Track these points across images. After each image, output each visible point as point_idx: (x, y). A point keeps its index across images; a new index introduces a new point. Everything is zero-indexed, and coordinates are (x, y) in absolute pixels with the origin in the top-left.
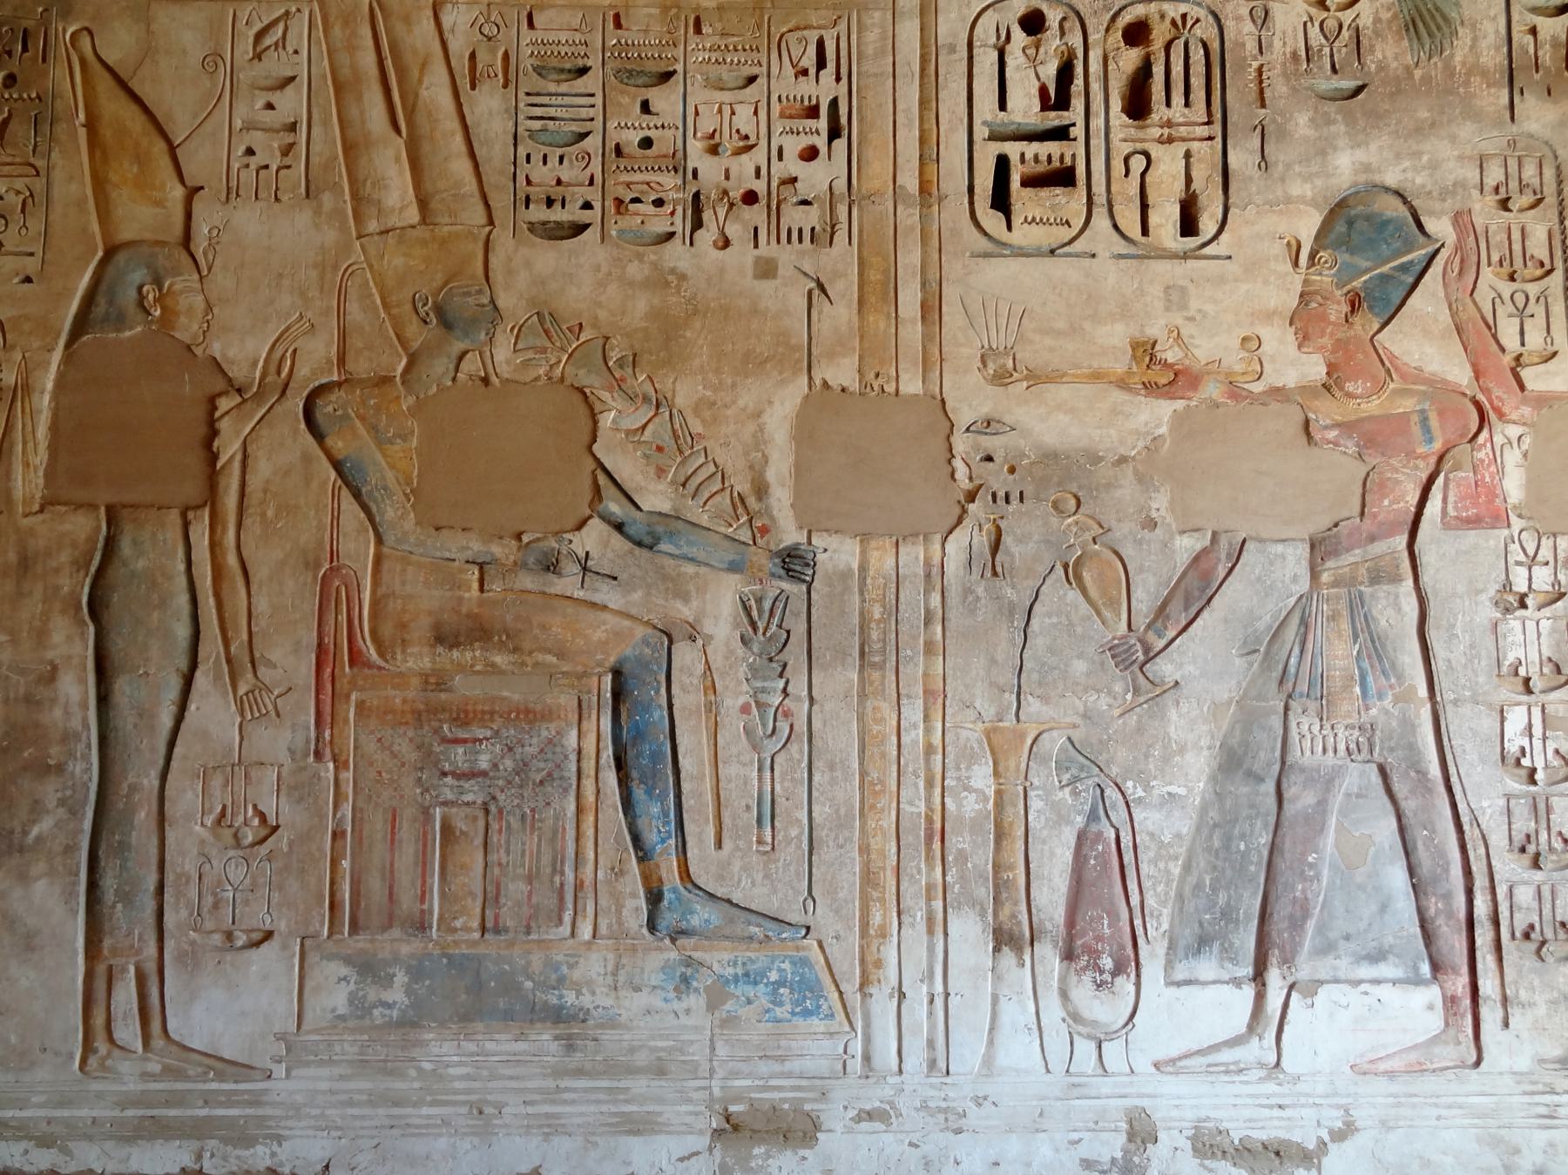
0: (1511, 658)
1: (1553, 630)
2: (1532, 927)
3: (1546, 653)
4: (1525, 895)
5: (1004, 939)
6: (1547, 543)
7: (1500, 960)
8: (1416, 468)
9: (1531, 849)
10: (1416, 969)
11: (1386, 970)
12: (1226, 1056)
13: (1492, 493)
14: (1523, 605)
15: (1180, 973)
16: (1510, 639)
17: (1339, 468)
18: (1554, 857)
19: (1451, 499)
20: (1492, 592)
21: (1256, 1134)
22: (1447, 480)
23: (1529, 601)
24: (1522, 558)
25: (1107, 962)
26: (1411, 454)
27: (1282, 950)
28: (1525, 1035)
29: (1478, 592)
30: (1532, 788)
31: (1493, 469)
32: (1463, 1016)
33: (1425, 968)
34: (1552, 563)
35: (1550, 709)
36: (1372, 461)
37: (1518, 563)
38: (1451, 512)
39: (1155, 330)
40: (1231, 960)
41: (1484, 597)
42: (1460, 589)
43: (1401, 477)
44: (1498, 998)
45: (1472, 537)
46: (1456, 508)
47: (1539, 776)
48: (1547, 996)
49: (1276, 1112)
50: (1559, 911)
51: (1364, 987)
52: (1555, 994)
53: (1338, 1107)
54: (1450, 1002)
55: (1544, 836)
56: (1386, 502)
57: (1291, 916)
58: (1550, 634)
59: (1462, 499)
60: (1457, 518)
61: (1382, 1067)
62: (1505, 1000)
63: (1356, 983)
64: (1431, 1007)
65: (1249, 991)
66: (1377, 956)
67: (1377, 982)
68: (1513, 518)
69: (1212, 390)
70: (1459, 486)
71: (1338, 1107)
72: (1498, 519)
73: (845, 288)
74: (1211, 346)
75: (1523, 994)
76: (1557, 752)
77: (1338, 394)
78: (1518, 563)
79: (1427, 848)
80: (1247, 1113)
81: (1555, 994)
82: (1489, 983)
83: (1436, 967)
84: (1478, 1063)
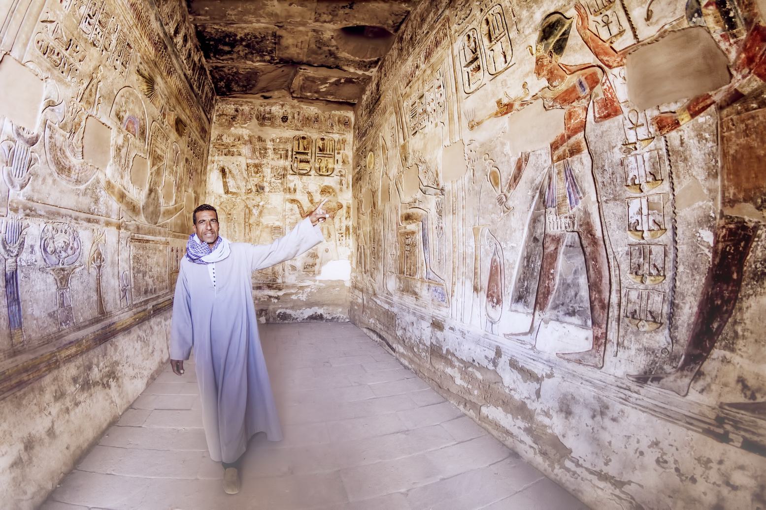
0: (631, 176)
1: (651, 158)
2: (635, 311)
3: (648, 170)
4: (633, 295)
5: (476, 289)
6: (641, 115)
7: (619, 325)
8: (582, 103)
9: (640, 272)
10: (586, 322)
11: (575, 320)
12: (522, 338)
13: (612, 101)
14: (636, 149)
15: (513, 308)
16: (630, 167)
17: (559, 114)
18: (652, 278)
19: (596, 110)
20: (620, 145)
21: (525, 366)
22: (593, 102)
23: (637, 146)
24: (631, 126)
25: (495, 300)
26: (578, 98)
27: (540, 305)
28: (623, 361)
29: (613, 147)
30: (642, 241)
31: (611, 90)
32: (599, 346)
33: (590, 323)
34: (645, 124)
35: (651, 199)
36: (567, 107)
37: (630, 129)
38: (597, 116)
39: (501, 96)
40: (527, 306)
41: (616, 150)
42: (605, 148)
43: (576, 109)
44: (615, 342)
45: (607, 123)
46: (599, 113)
47: (645, 235)
48: (637, 346)
49: (532, 361)
50: (649, 306)
51: (565, 325)
52: (641, 347)
53: (550, 366)
54: (596, 338)
55: (647, 266)
56: (572, 121)
57: (544, 293)
58: (649, 160)
59: (600, 108)
60: (600, 117)
61: (567, 357)
62: (618, 344)
63: (562, 322)
64: (587, 339)
65: (530, 318)
66: (572, 313)
67: (570, 324)
68: (624, 109)
69: (517, 105)
70: (598, 103)
71: (550, 366)
72: (616, 112)
73: (446, 122)
74: (514, 92)
75: (626, 343)
76: (654, 221)
77: (551, 88)
78: (630, 129)
79: (594, 270)
80: (524, 358)
81: (641, 347)
82: (612, 334)
83: (593, 323)
84: (602, 367)
